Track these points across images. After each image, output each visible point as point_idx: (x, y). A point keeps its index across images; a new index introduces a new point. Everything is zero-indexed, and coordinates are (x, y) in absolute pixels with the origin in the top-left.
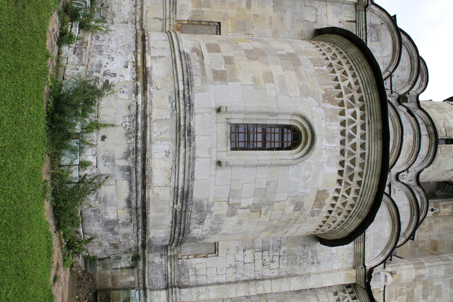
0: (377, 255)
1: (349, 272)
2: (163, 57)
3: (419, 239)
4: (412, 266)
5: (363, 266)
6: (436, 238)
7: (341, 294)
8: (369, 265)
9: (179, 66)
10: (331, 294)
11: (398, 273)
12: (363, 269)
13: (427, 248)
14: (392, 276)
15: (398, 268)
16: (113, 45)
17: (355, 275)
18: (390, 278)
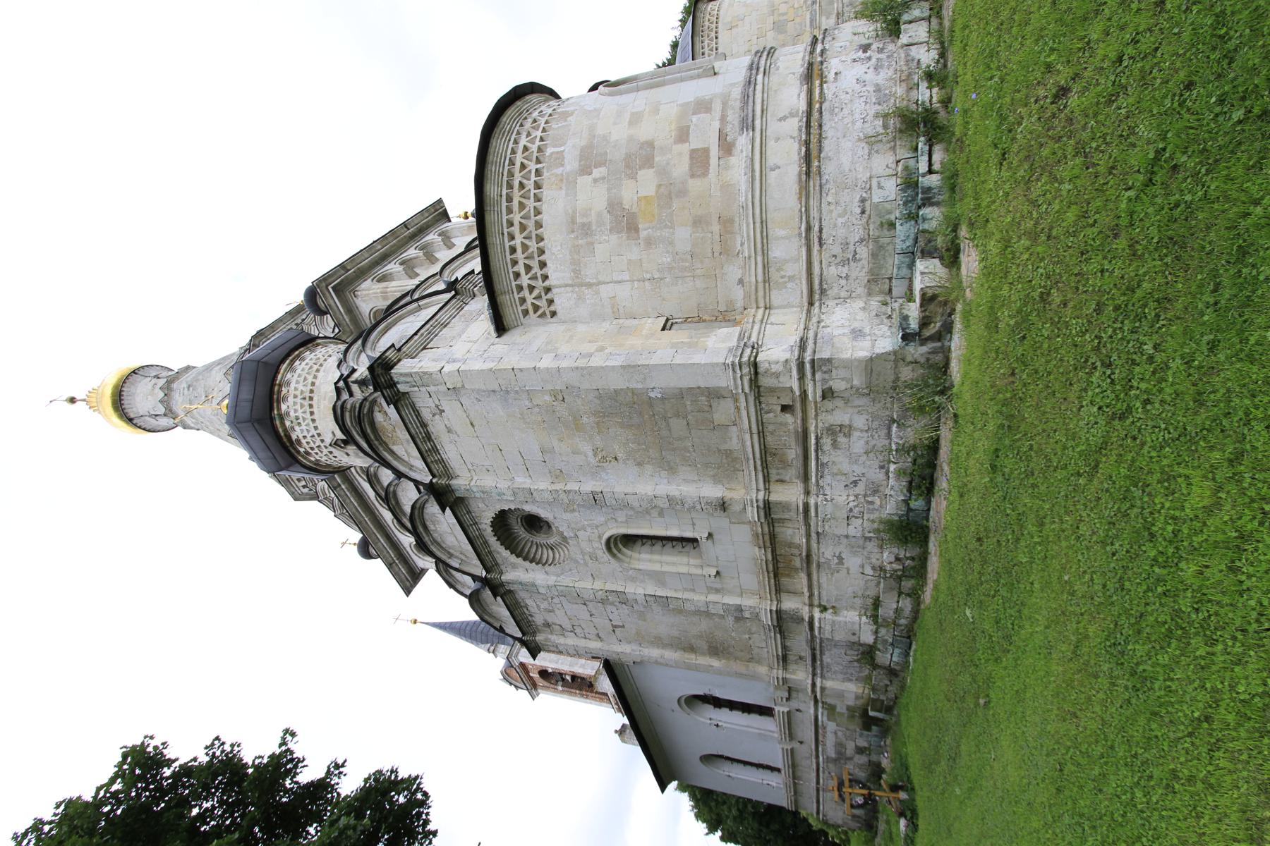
2: (780, 120)
9: (758, 101)
16: (859, 106)
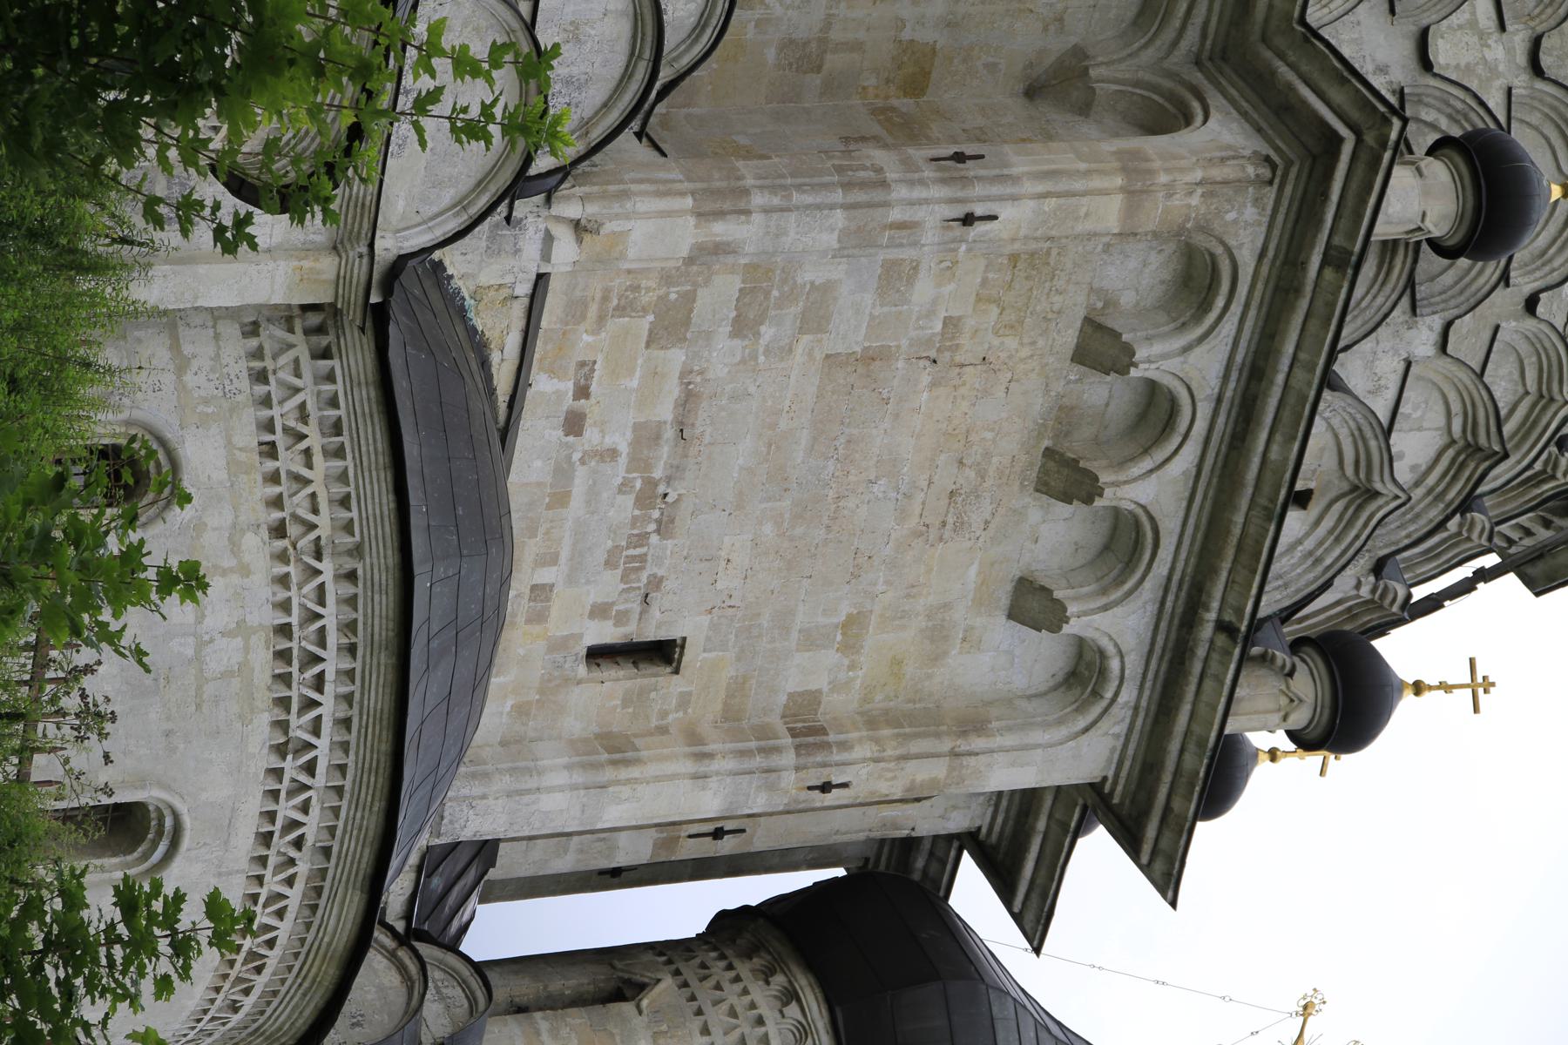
0: (435, 209)
1: (306, 264)
3: (835, 35)
4: (689, 202)
5: (364, 250)
6: (926, 35)
7: (273, 334)
8: (388, 246)
10: (231, 330)
11: (609, 227)
12: (365, 260)
13: (871, 81)
14: (580, 241)
15: (616, 208)
17: (331, 275)
18: (566, 250)
